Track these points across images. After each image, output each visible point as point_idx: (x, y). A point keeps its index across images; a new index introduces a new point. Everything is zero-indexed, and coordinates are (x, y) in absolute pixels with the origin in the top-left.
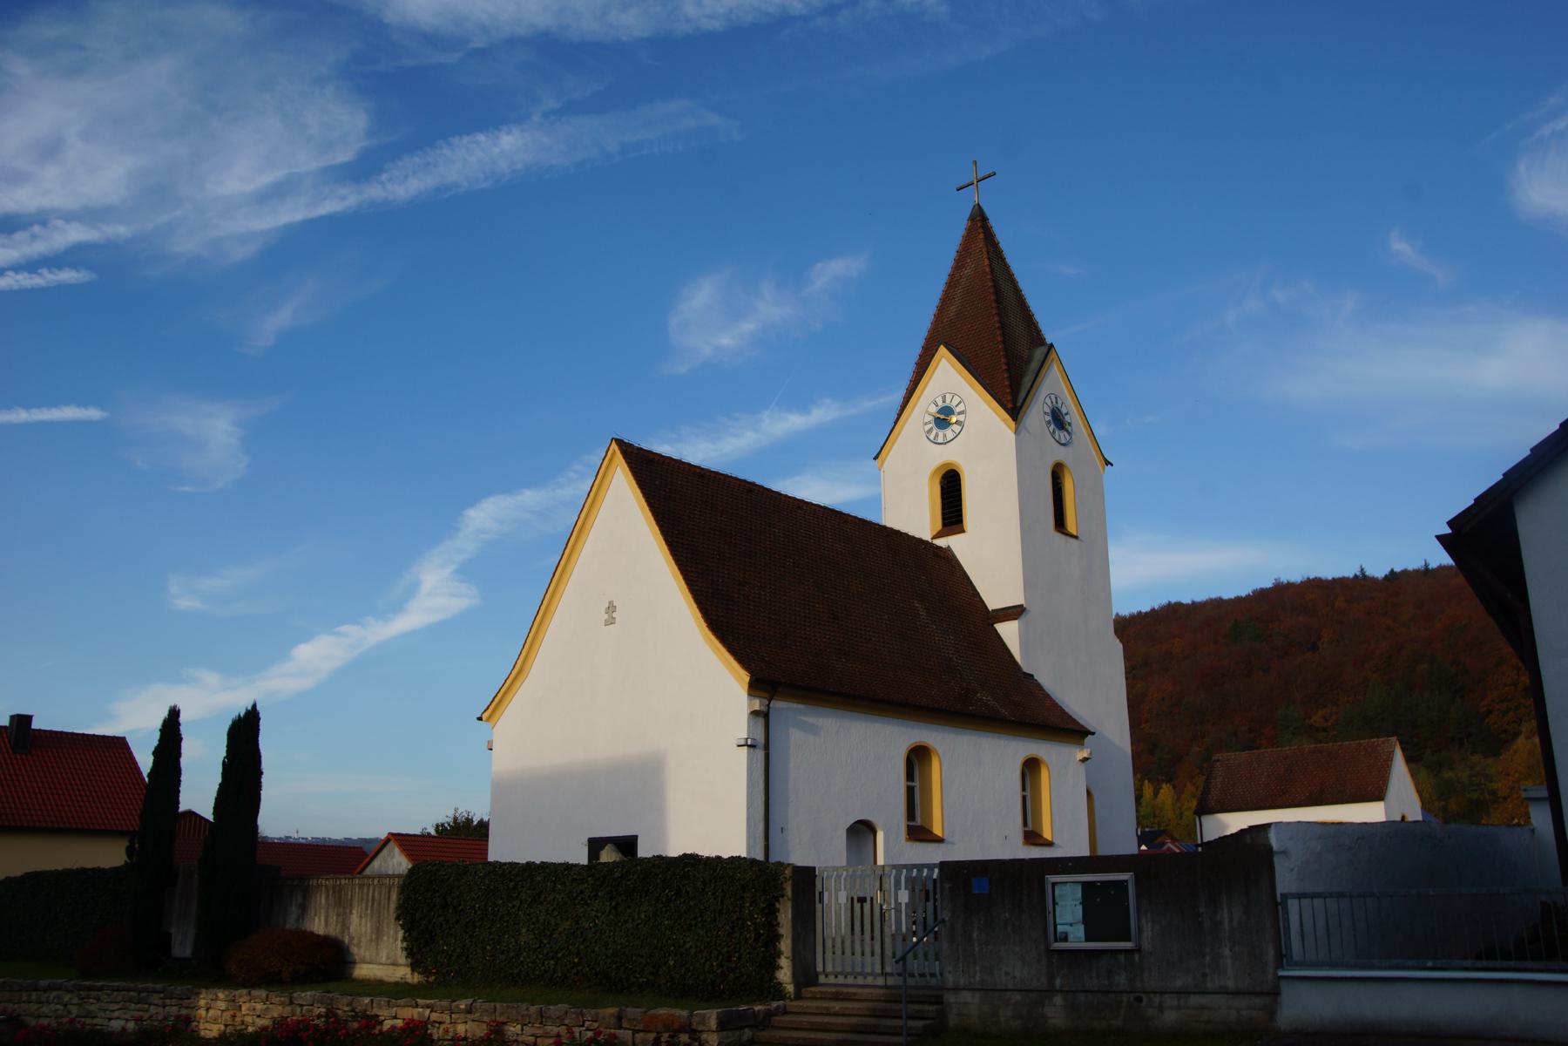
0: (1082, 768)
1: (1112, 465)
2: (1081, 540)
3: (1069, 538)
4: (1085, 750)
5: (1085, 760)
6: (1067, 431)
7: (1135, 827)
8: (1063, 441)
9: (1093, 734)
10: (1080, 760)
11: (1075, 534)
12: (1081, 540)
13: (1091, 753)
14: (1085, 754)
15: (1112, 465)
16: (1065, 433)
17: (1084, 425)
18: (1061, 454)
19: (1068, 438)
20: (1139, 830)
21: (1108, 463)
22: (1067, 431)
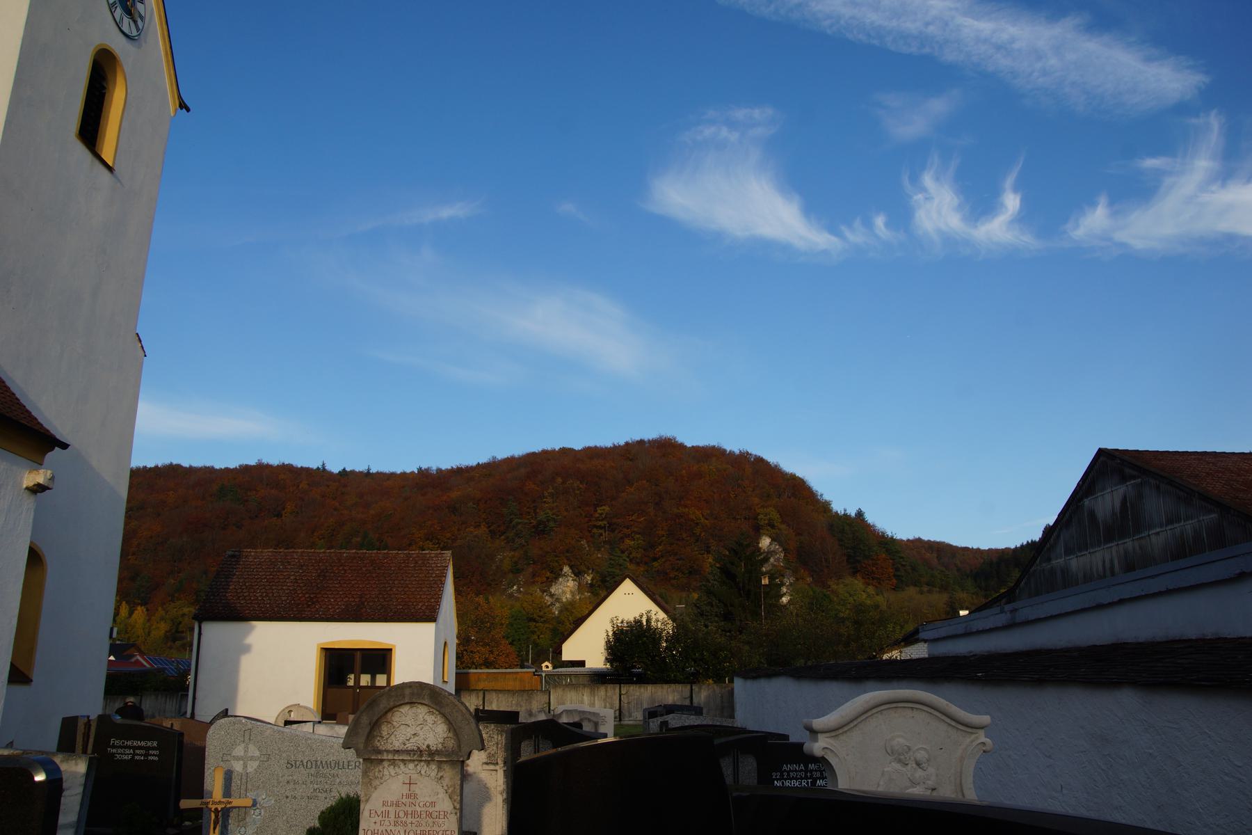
0: (29, 502)
1: (188, 110)
2: (116, 177)
3: (97, 163)
4: (42, 471)
5: (38, 489)
6: (135, 22)
7: (110, 624)
8: (125, 29)
9: (64, 446)
10: (27, 488)
11: (110, 164)
12: (116, 177)
13: (52, 479)
14: (40, 477)
15: (188, 110)
16: (132, 23)
17: (163, 34)
18: (118, 44)
19: (135, 33)
20: (115, 630)
21: (183, 106)
22: (135, 22)
